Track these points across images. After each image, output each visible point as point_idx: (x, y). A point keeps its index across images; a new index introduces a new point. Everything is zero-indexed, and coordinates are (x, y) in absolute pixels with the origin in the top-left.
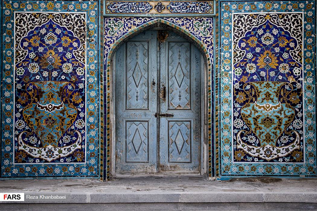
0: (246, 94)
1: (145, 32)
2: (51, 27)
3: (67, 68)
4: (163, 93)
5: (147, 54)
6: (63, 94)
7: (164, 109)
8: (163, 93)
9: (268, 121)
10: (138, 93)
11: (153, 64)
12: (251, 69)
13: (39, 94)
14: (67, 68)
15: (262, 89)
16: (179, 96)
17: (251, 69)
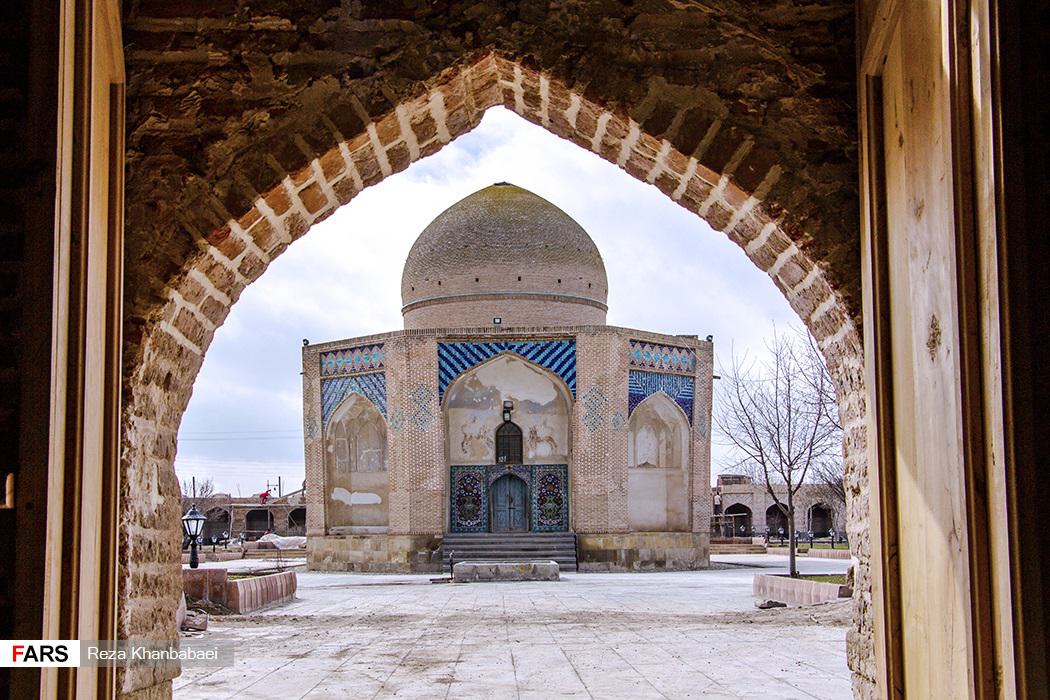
0: (542, 501)
1: (504, 476)
2: (469, 476)
3: (475, 491)
4: (511, 500)
5: (505, 484)
6: (474, 502)
7: (512, 506)
8: (511, 500)
9: (550, 510)
10: (502, 499)
11: (508, 489)
12: (544, 491)
13: (465, 501)
14: (475, 491)
15: (548, 498)
16: (518, 500)
17: (544, 491)
